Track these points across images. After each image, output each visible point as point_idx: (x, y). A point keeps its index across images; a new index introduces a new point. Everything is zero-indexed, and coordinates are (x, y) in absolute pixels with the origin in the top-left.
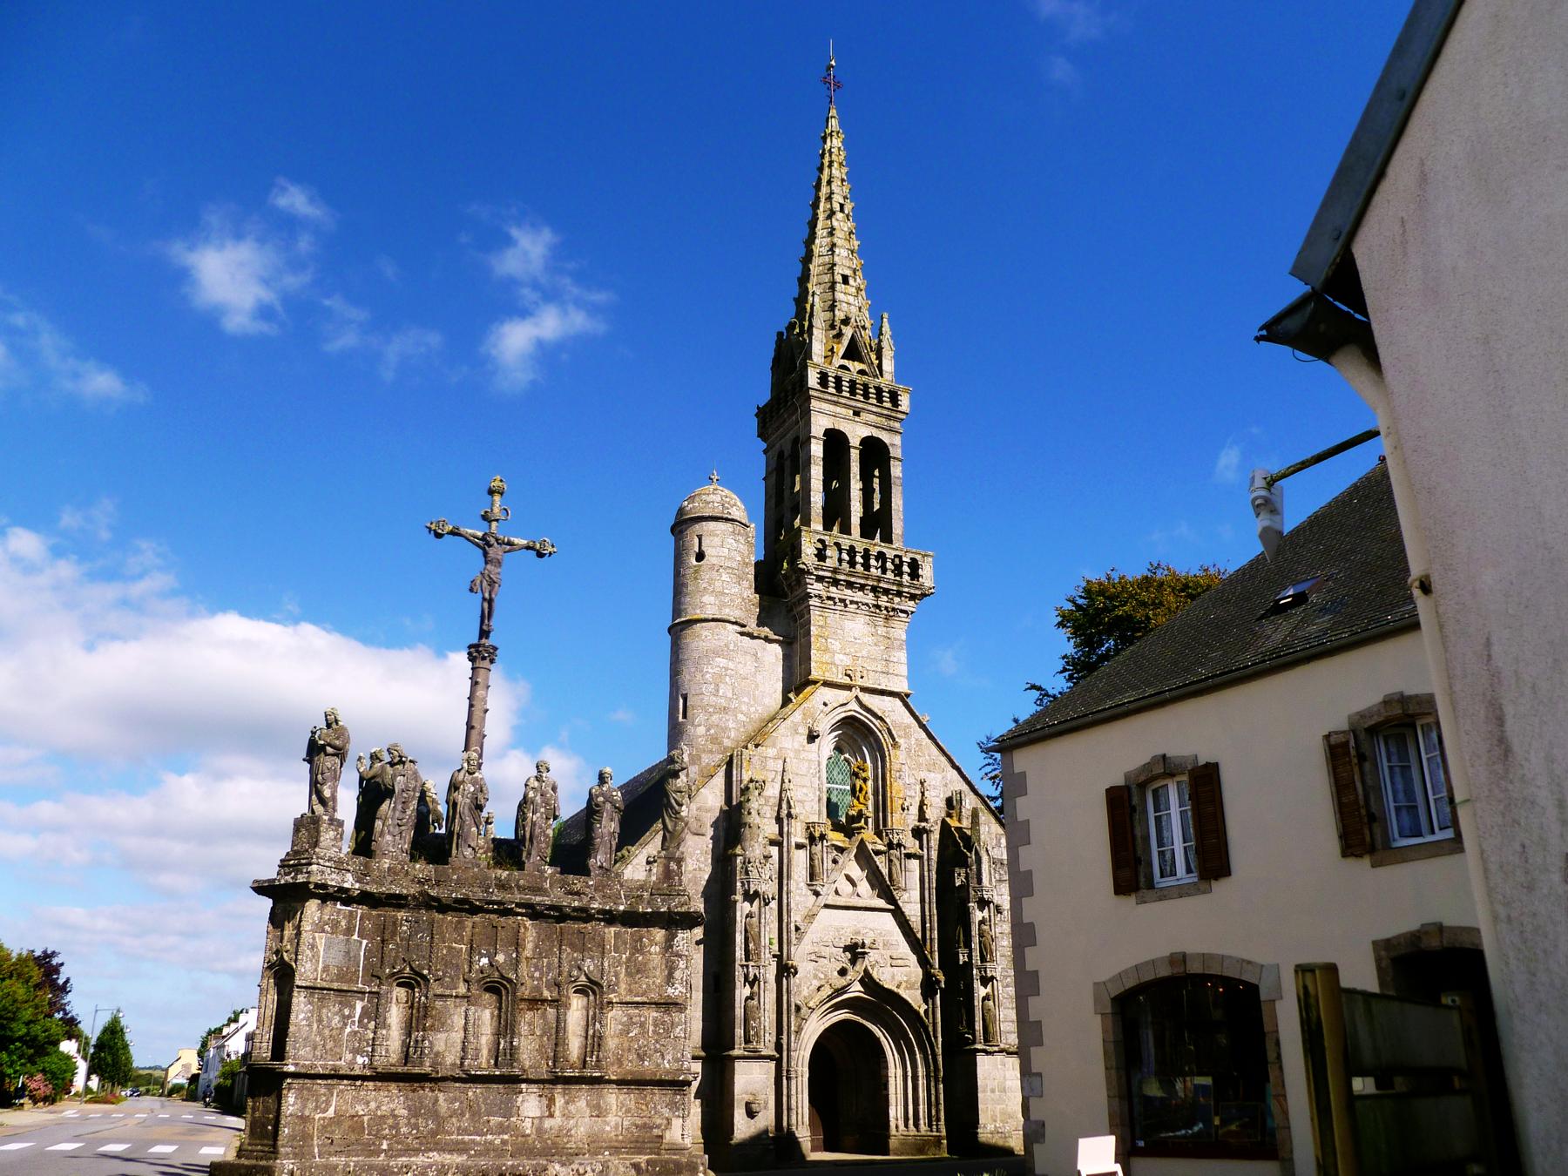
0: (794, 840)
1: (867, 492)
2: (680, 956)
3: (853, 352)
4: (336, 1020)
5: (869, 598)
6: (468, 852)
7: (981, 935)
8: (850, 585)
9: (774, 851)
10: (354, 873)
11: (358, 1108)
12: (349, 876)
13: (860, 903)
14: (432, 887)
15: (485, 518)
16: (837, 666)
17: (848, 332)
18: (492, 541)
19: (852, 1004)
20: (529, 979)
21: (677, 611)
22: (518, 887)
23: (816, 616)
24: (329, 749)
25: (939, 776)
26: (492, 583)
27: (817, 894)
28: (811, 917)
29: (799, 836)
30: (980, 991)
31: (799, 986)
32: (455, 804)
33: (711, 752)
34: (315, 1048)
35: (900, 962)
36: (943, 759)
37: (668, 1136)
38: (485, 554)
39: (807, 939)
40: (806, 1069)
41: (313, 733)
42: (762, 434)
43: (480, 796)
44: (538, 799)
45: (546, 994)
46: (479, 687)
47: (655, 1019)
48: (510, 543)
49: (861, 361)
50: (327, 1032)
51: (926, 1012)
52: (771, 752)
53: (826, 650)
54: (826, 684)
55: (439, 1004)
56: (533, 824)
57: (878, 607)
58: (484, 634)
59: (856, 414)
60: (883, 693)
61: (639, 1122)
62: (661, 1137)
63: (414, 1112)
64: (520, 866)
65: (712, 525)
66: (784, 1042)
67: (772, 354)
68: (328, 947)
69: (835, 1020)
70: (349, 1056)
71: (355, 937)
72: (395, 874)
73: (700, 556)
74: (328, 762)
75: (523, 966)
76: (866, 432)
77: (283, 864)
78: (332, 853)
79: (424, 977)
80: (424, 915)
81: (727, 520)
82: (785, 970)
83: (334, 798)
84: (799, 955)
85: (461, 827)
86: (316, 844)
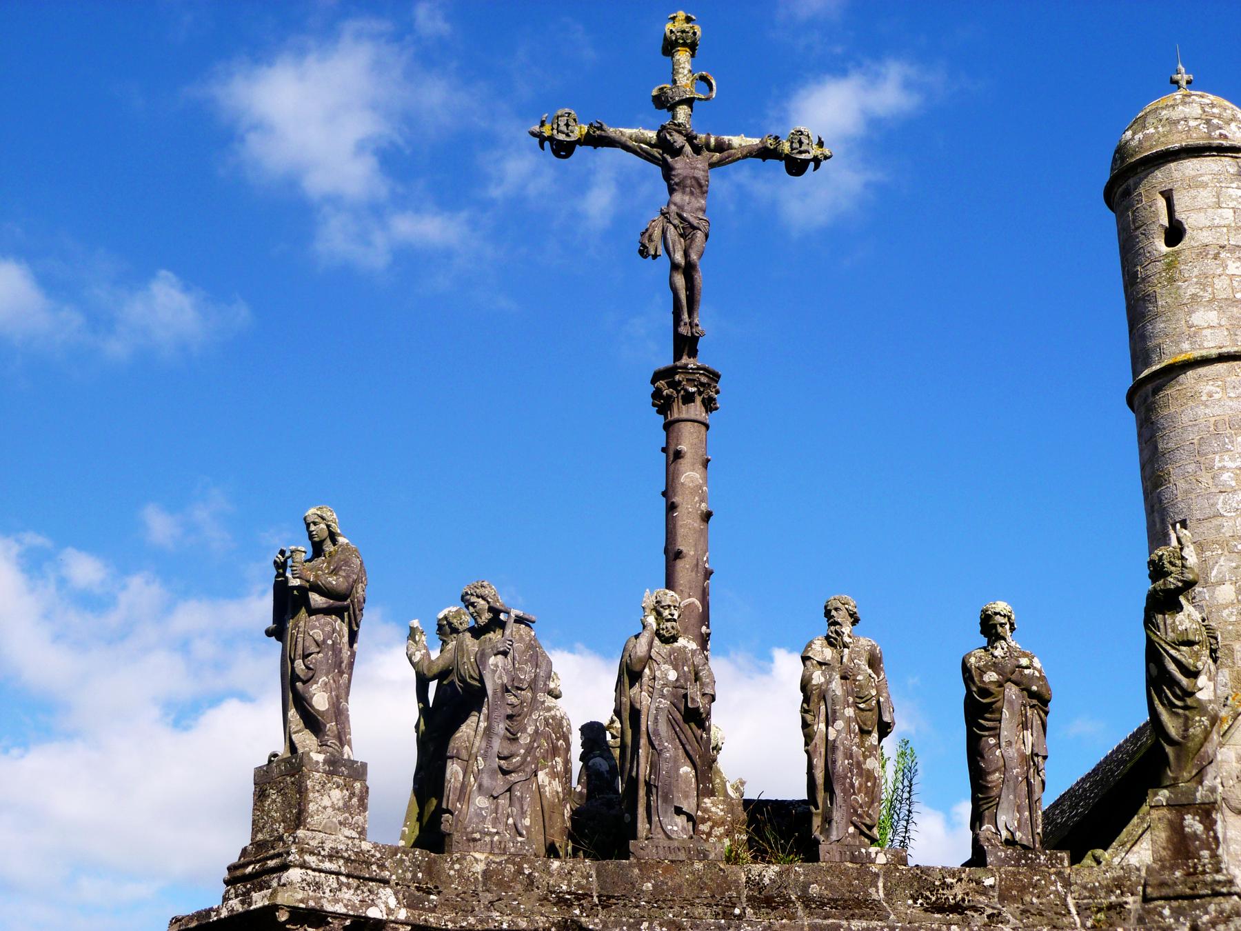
6: (677, 826)
10: (399, 887)
12: (388, 896)
14: (591, 911)
15: (663, 102)
18: (679, 140)
21: (1140, 352)
22: (807, 901)
24: (316, 599)
26: (688, 230)
32: (635, 714)
38: (668, 171)
41: (281, 566)
43: (693, 691)
44: (837, 687)
46: (684, 464)
48: (721, 147)
56: (831, 747)
58: (685, 344)
64: (810, 852)
65: (1190, 166)
72: (501, 884)
73: (1175, 233)
74: (314, 629)
77: (236, 878)
78: (342, 839)
81: (1221, 150)
83: (339, 712)
85: (654, 766)
86: (298, 820)
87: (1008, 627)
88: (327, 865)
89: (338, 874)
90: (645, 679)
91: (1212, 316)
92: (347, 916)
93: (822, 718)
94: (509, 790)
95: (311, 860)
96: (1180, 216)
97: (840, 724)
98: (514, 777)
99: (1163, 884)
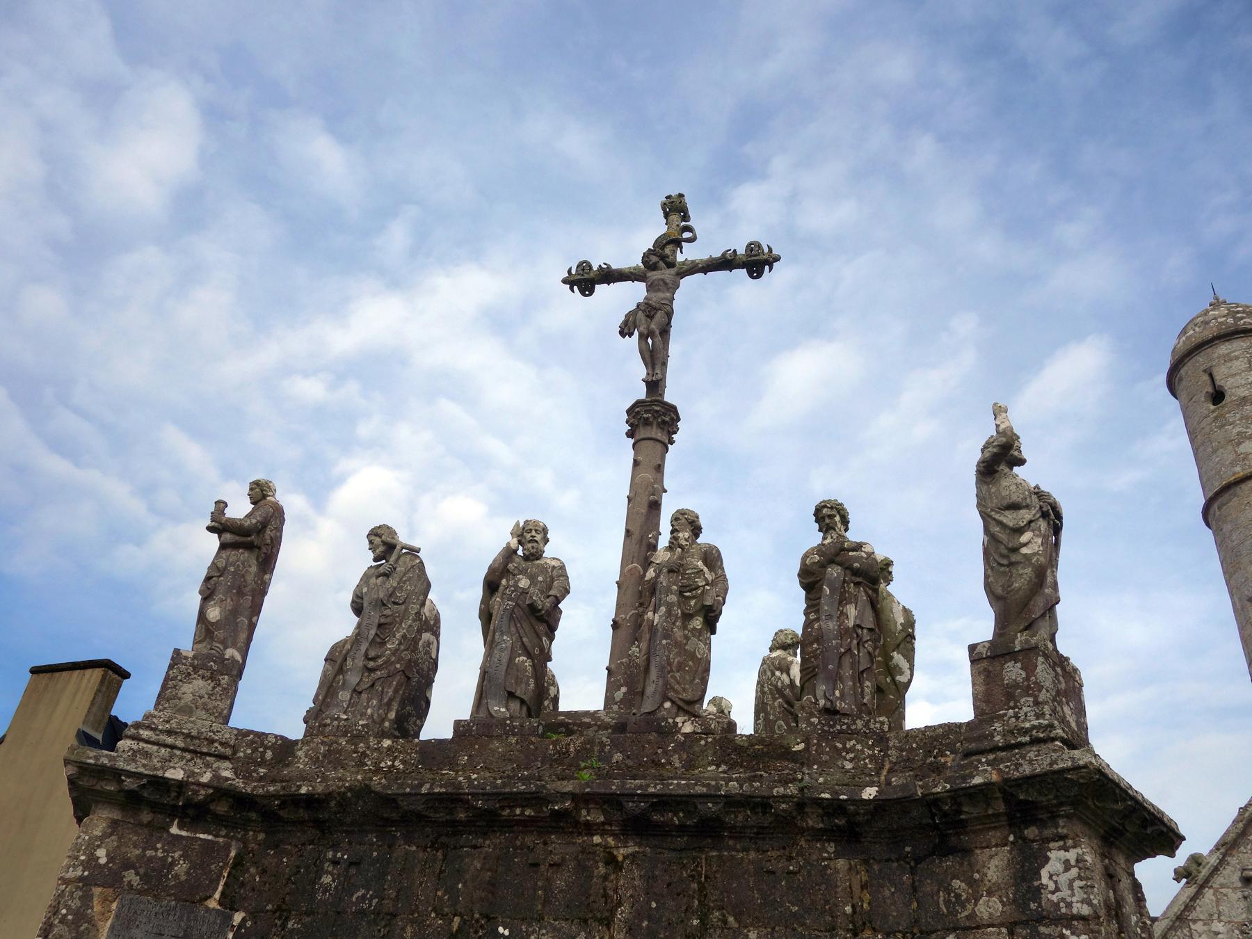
71: (213, 904)
87: (837, 518)
89: (173, 747)
90: (501, 588)
93: (651, 608)
94: (373, 685)
96: (1218, 383)
97: (663, 609)
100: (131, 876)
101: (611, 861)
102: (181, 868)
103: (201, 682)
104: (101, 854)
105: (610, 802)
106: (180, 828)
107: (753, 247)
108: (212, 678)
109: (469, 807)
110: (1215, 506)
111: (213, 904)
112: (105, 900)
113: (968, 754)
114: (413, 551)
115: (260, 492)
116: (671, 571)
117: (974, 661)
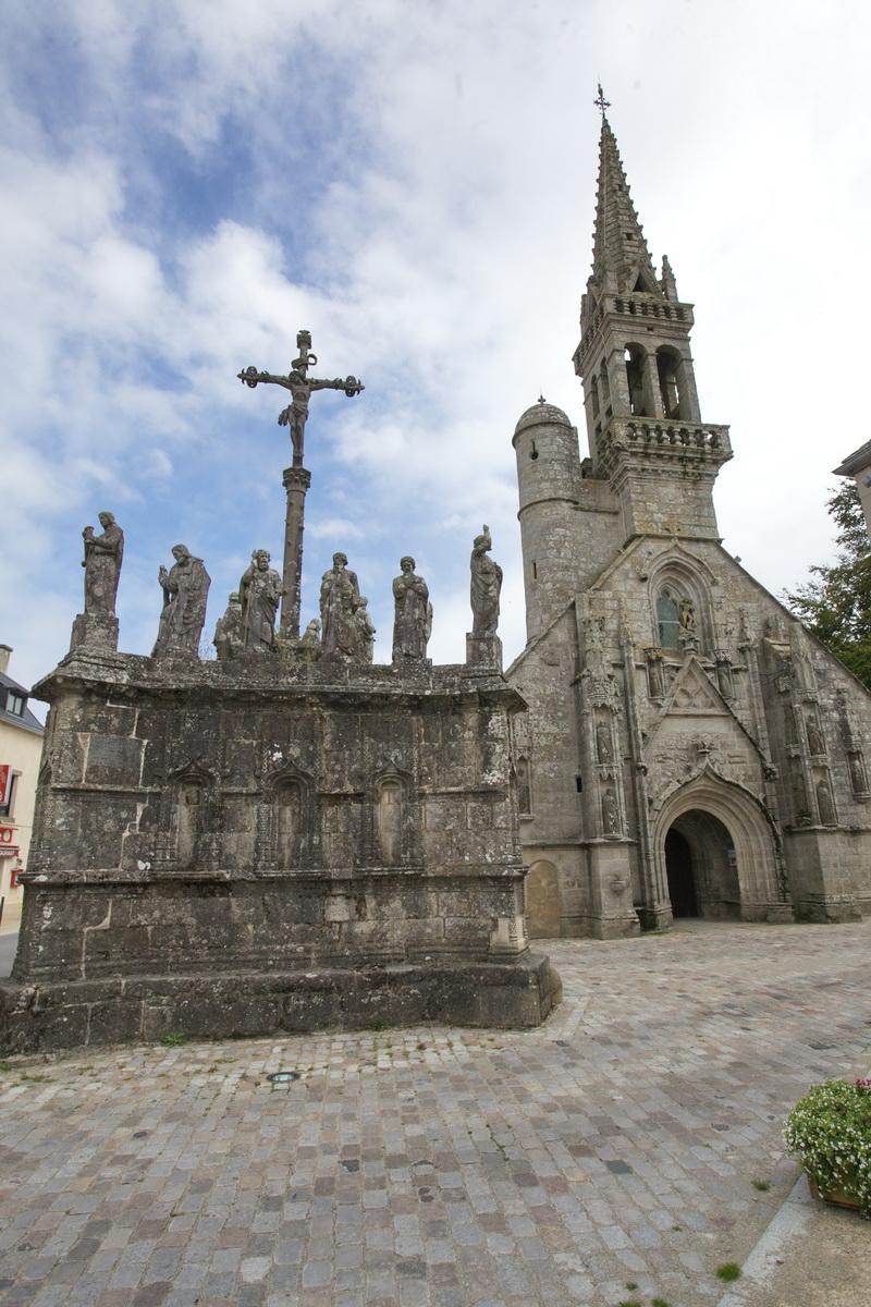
0: (633, 664)
1: (666, 400)
2: (497, 740)
3: (639, 287)
4: (109, 825)
5: (678, 468)
7: (810, 730)
8: (660, 456)
9: (618, 674)
11: (140, 917)
13: (697, 712)
16: (656, 523)
17: (635, 270)
19: (700, 795)
20: (331, 774)
23: (634, 487)
24: (98, 549)
25: (755, 605)
27: (659, 706)
28: (654, 726)
29: (636, 658)
30: (814, 779)
31: (650, 783)
33: (558, 601)
34: (80, 855)
35: (737, 759)
36: (756, 591)
37: (495, 938)
39: (653, 744)
40: (663, 852)
42: (579, 372)
45: (349, 788)
47: (473, 810)
49: (651, 292)
50: (96, 837)
51: (765, 799)
52: (608, 594)
53: (646, 511)
54: (649, 536)
55: (229, 804)
57: (685, 473)
58: (298, 459)
59: (650, 329)
60: (698, 540)
61: (463, 922)
62: (488, 939)
63: (204, 920)
65: (542, 430)
66: (641, 830)
67: (580, 312)
68: (95, 747)
69: (684, 810)
70: (126, 862)
71: (133, 736)
75: (322, 764)
76: (659, 343)
79: (211, 776)
80: (208, 710)
81: (553, 424)
82: (636, 769)
84: (645, 757)
88: (92, 660)
89: (97, 664)
91: (548, 485)
92: (94, 681)
95: (85, 659)
97: (334, 605)
98: (191, 626)
99: (468, 672)
100: (93, 726)
101: (322, 717)
102: (116, 722)
103: (101, 630)
104: (77, 717)
105: (323, 695)
106: (111, 702)
107: (351, 378)
108: (107, 628)
109: (256, 695)
110: (525, 512)
111: (133, 736)
112: (84, 738)
113: (463, 678)
114: (199, 561)
115: (107, 521)
116: (337, 586)
117: (468, 640)
